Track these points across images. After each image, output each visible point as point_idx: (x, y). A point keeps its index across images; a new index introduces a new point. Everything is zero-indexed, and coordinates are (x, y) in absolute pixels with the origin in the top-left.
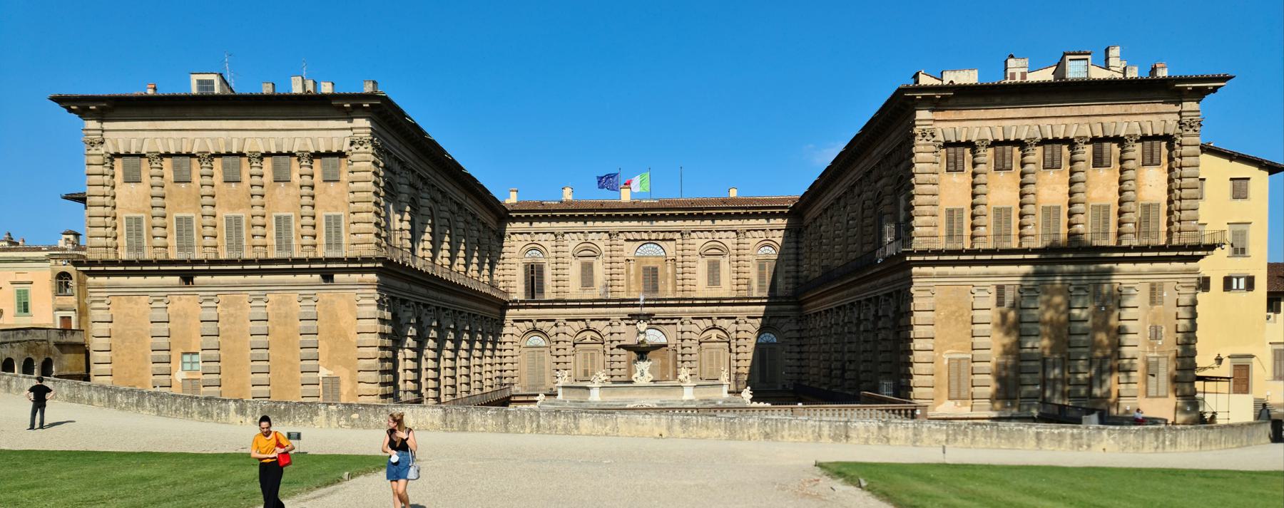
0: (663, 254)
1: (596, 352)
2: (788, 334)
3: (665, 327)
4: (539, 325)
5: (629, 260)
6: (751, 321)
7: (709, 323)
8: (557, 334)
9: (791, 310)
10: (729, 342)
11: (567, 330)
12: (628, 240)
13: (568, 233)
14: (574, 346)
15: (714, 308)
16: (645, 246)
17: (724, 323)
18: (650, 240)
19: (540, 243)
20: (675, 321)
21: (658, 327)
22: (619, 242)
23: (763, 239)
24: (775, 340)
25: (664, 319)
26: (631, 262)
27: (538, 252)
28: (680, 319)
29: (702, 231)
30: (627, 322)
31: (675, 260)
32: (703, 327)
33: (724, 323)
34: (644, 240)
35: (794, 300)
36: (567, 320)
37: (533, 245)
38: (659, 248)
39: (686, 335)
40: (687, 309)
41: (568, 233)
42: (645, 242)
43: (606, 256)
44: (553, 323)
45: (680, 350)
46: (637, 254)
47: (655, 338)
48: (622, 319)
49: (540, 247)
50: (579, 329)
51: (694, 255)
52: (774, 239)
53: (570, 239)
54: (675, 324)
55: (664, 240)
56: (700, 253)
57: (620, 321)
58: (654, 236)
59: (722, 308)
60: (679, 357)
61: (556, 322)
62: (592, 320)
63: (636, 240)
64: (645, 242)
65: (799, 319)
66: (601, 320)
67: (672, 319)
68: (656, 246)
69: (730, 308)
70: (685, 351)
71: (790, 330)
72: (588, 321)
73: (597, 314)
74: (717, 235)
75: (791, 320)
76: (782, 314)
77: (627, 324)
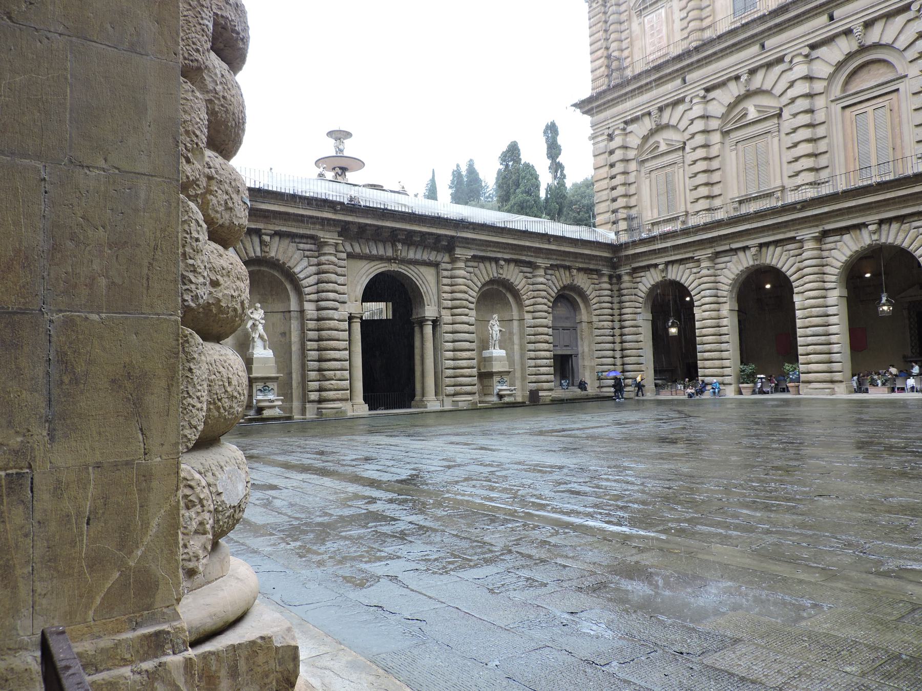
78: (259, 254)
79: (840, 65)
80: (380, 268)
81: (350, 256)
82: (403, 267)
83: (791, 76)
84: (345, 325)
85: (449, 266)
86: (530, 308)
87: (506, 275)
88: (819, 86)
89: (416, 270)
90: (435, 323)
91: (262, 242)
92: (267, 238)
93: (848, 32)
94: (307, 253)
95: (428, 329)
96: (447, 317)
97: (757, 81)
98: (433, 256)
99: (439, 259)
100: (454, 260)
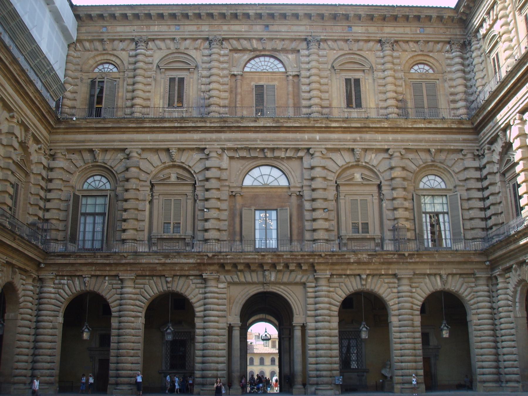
0: (283, 70)
1: (183, 198)
2: (463, 176)
3: (285, 163)
4: (100, 158)
5: (234, 75)
6: (411, 156)
7: (348, 158)
8: (127, 169)
9: (464, 141)
10: (379, 186)
11: (144, 165)
12: (235, 50)
13: (153, 40)
14: (151, 190)
15: (357, 136)
16: (257, 60)
17: (373, 159)
18: (264, 50)
19: (115, 53)
20: (300, 154)
21: (276, 163)
23: (416, 53)
24: (443, 186)
26: (239, 77)
27: (111, 67)
28: (308, 149)
29: (335, 41)
30: (232, 154)
31: (298, 76)
32: (341, 162)
34: (254, 50)
35: (469, 126)
36: (143, 150)
37: (106, 57)
38: (276, 62)
40: (318, 136)
41: (153, 40)
42: (258, 53)
43: (203, 69)
44: (120, 156)
45: (307, 194)
46: (246, 69)
47: (271, 179)
48: (223, 149)
49: (114, 59)
50: (159, 163)
52: (431, 54)
53: (155, 48)
54: (301, 158)
55: (285, 51)
56: (333, 67)
57: (220, 152)
58: (269, 46)
59: (367, 136)
60: (307, 205)
61: (127, 152)
62: (181, 150)
63: (244, 50)
64: (258, 53)
65: (476, 153)
66: (192, 149)
67: (298, 150)
68: (272, 60)
69: (379, 137)
70: (315, 195)
71: (466, 169)
72: (174, 152)
73: (186, 140)
74: (355, 47)
75: (465, 155)
76: (453, 146)
77: (231, 158)
78: (165, 288)
80: (254, 290)
81: (230, 283)
82: (274, 288)
84: (225, 332)
85: (313, 285)
86: (396, 312)
87: (371, 286)
89: (286, 289)
90: (304, 328)
91: (167, 282)
92: (169, 279)
94: (198, 285)
95: (298, 333)
96: (311, 324)
98: (299, 277)
99: (304, 280)
100: (316, 279)
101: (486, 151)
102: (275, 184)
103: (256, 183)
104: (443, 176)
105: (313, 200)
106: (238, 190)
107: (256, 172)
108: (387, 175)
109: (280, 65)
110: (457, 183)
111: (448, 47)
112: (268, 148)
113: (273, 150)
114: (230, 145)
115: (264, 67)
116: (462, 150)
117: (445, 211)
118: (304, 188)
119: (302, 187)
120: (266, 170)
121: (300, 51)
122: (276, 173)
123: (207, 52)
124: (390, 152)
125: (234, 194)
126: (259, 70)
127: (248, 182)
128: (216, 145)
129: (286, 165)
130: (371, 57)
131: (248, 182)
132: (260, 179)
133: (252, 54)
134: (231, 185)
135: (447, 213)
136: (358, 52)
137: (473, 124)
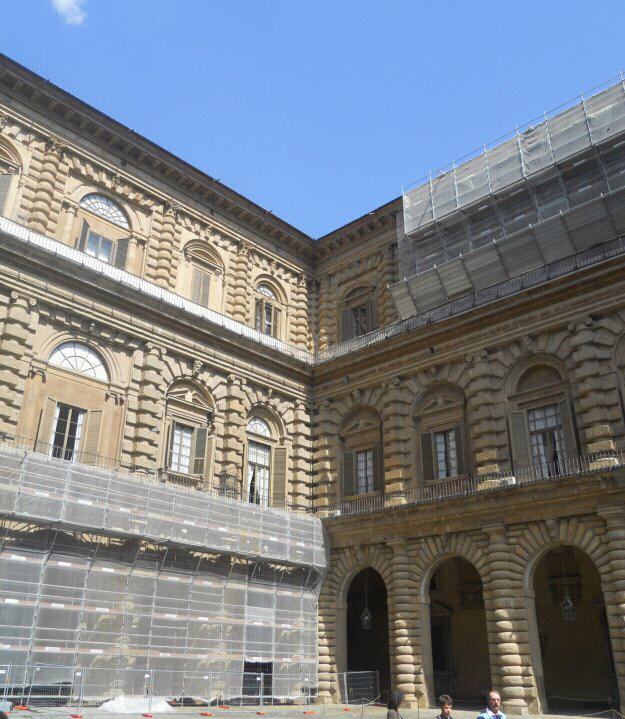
2: (291, 428)
10: (210, 416)
12: (75, 173)
17: (211, 380)
22: (62, 166)
23: (265, 272)
24: (268, 435)
25: (117, 333)
26: (71, 209)
33: (211, 380)
34: (101, 185)
39: (151, 375)
51: (177, 248)
52: (279, 280)
55: (135, 204)
67: (130, 338)
77: (43, 320)
79: (511, 368)
83: (472, 373)
88: (497, 385)
93: (518, 342)
97: (444, 375)
101: (322, 408)
102: (90, 374)
103: (65, 365)
104: (270, 423)
105: (140, 412)
106: (43, 366)
107: (68, 351)
108: (223, 404)
109: (123, 219)
110: (285, 435)
111: (295, 280)
112: (95, 321)
113: (101, 327)
114: (48, 298)
115: (105, 213)
116: (295, 399)
117: (267, 464)
118: (130, 392)
119: (127, 389)
120: (81, 352)
121: (154, 213)
122: (94, 359)
123: (41, 156)
124: (232, 376)
125: (35, 370)
126: (97, 212)
127: (56, 360)
128: (29, 291)
129: (106, 352)
130: (225, 256)
131: (56, 360)
132: (71, 360)
133: (93, 189)
134: (36, 357)
135: (268, 468)
136: (214, 245)
137: (313, 372)
